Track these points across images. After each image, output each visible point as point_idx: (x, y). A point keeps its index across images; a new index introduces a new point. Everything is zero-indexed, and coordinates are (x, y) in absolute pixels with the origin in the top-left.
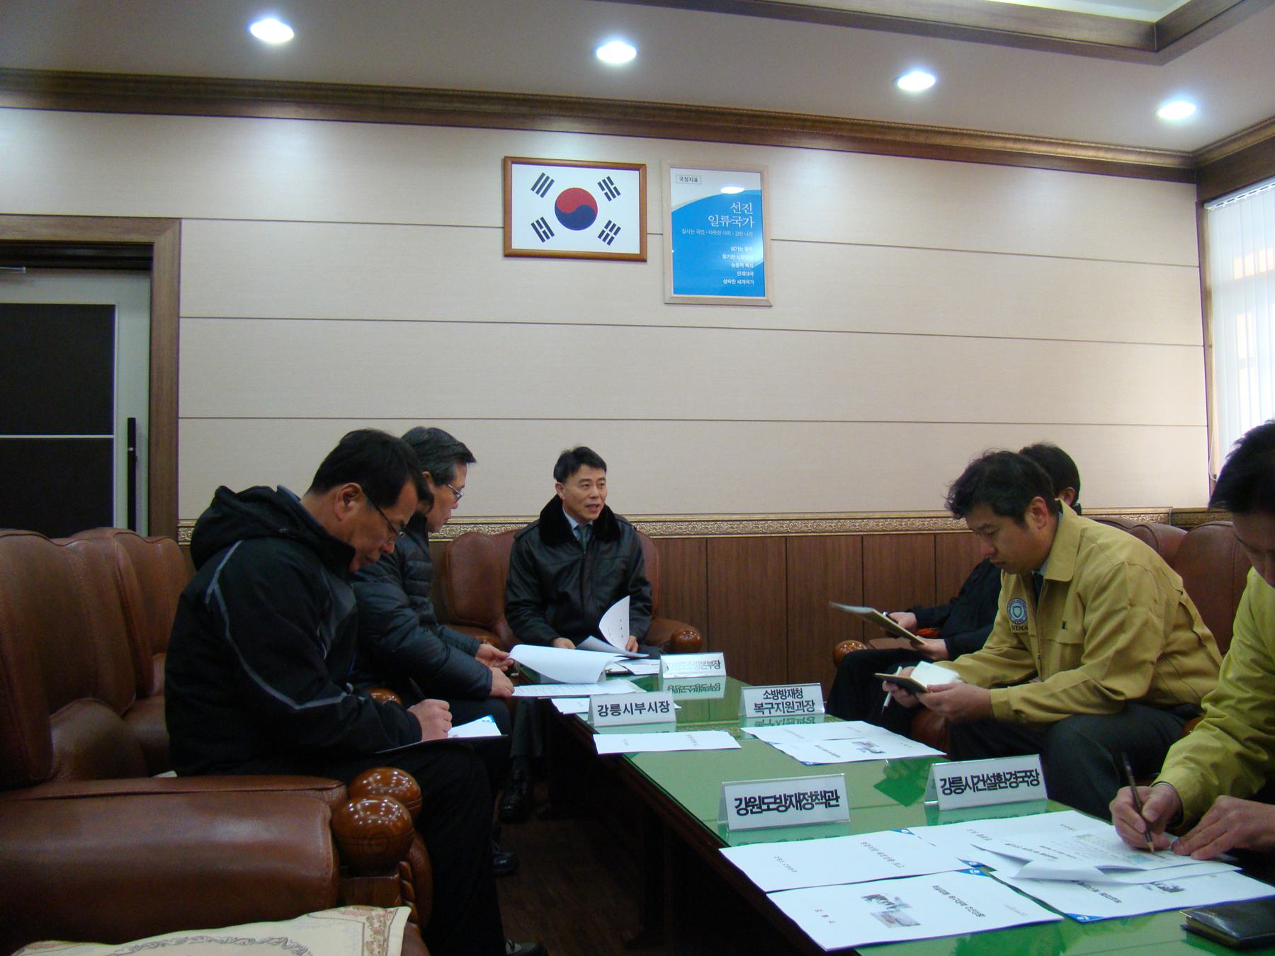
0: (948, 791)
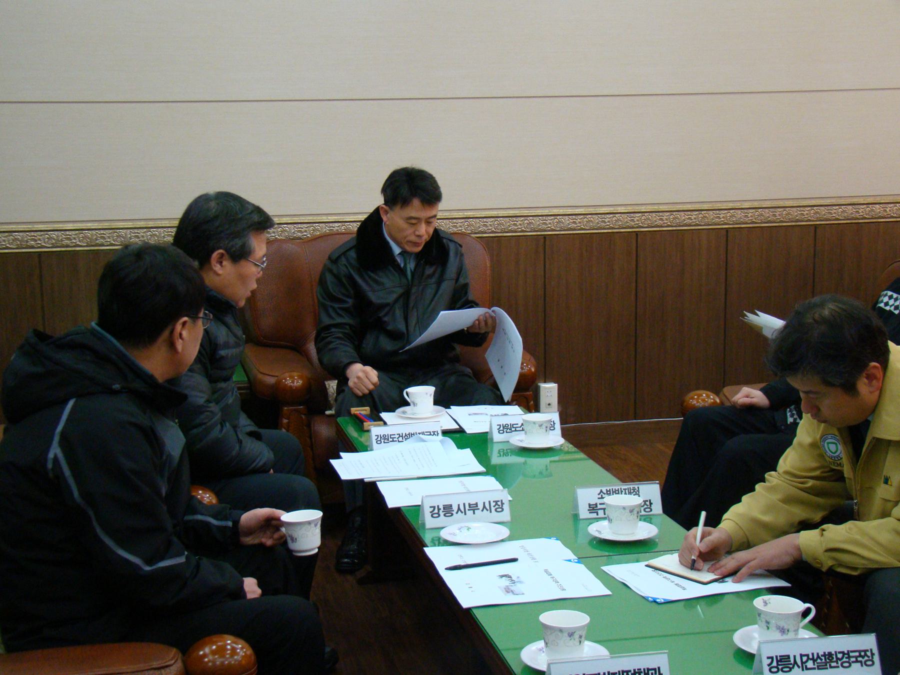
0: (775, 670)
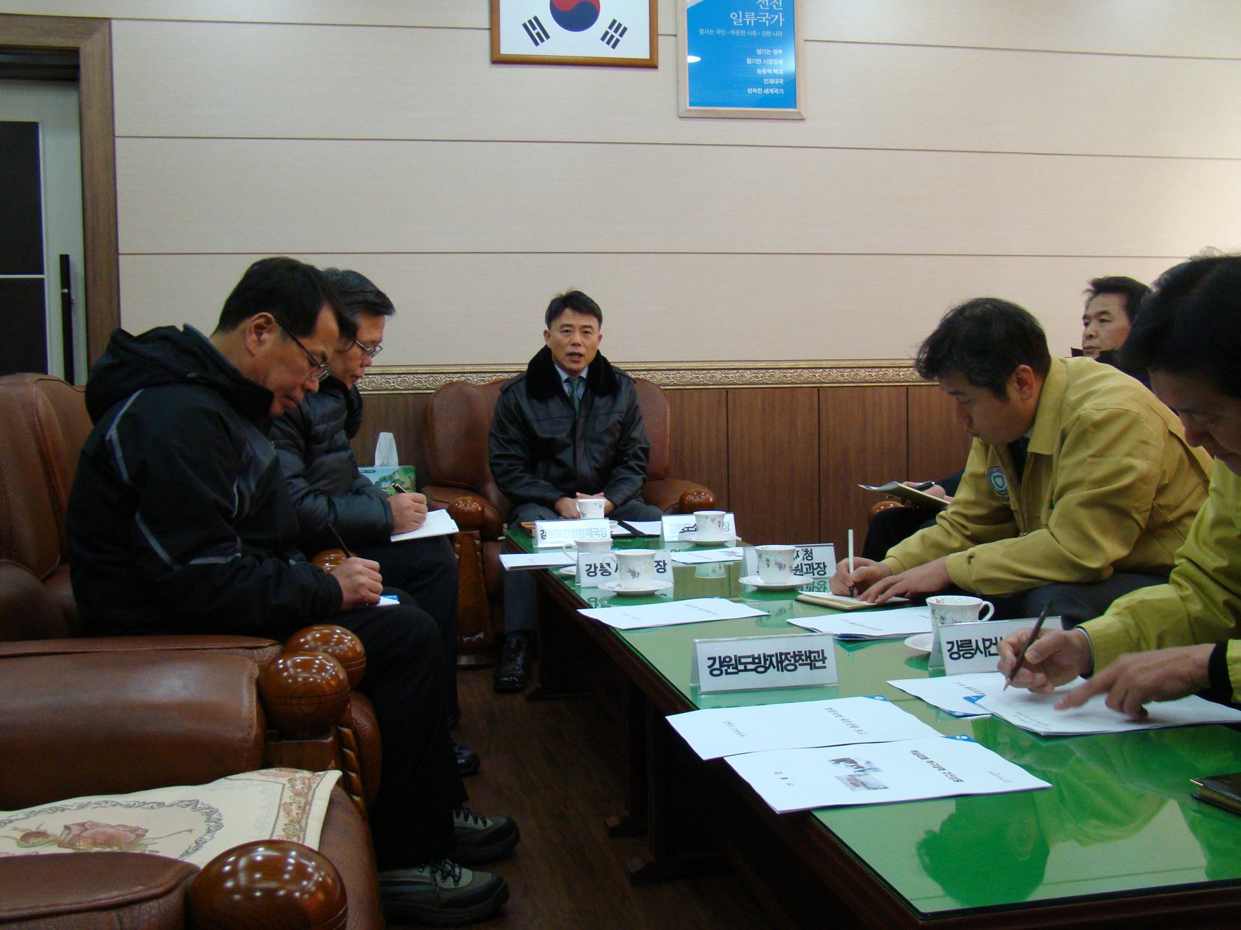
0: (955, 656)
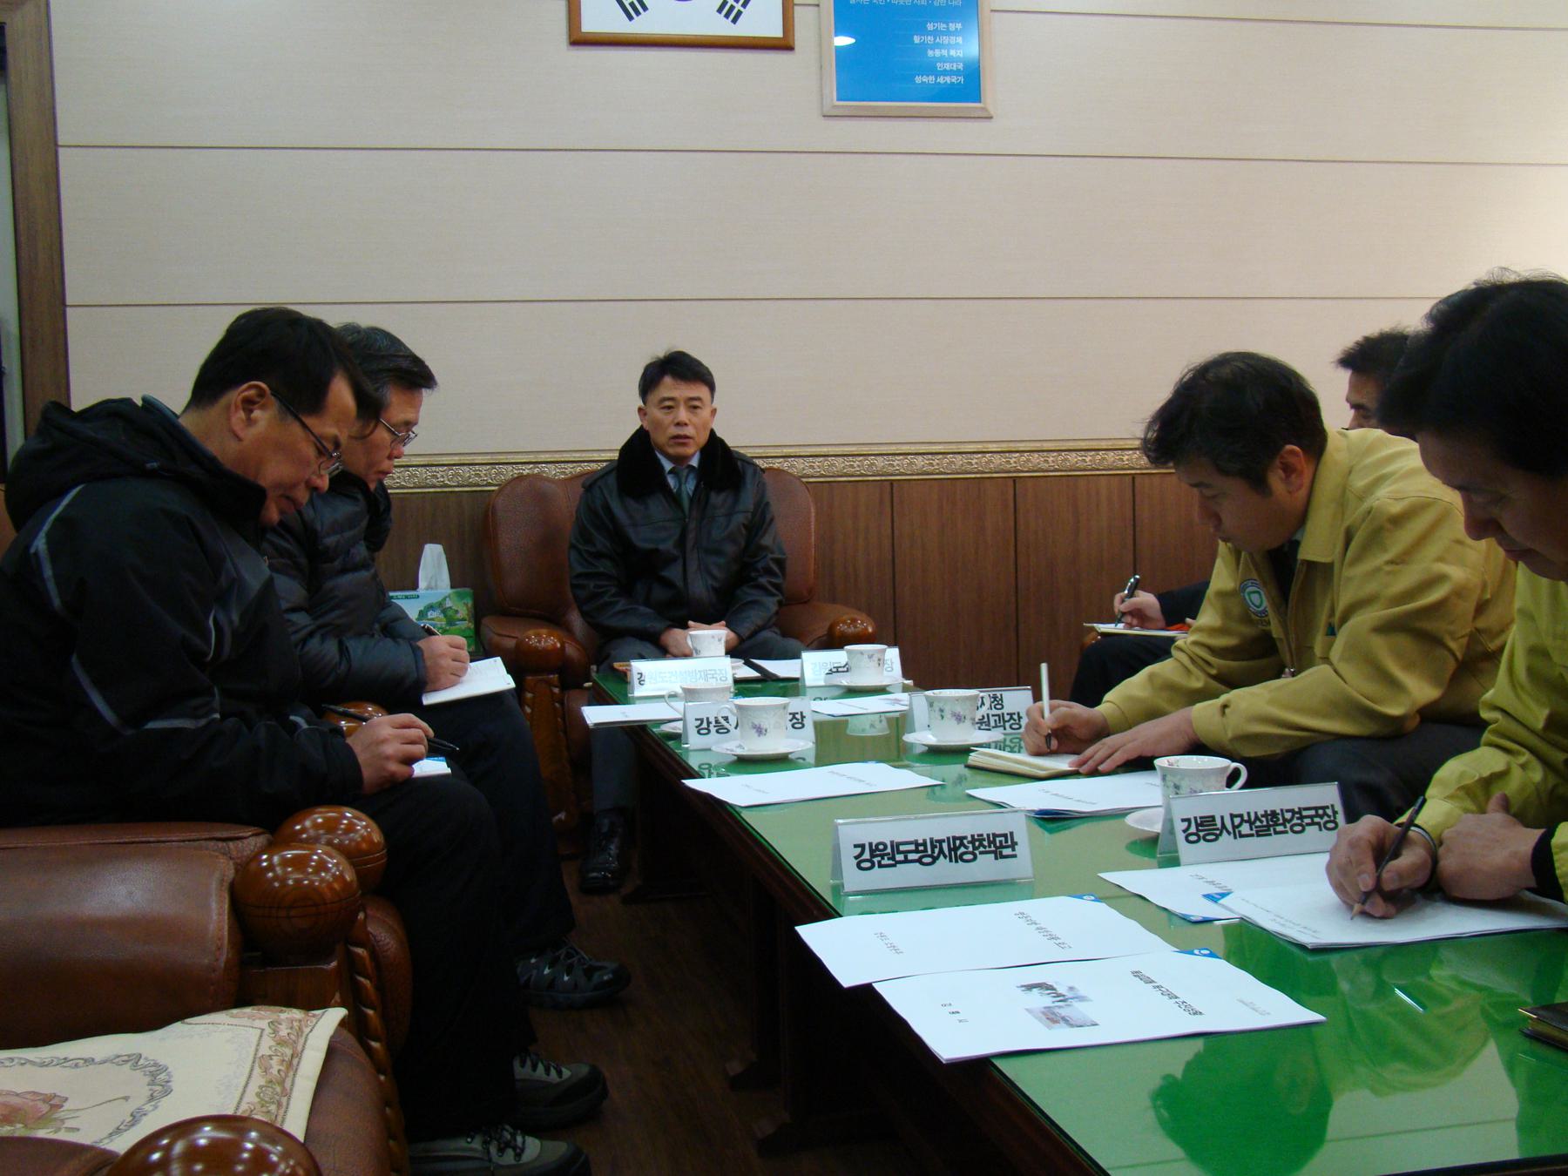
0: (1193, 838)
